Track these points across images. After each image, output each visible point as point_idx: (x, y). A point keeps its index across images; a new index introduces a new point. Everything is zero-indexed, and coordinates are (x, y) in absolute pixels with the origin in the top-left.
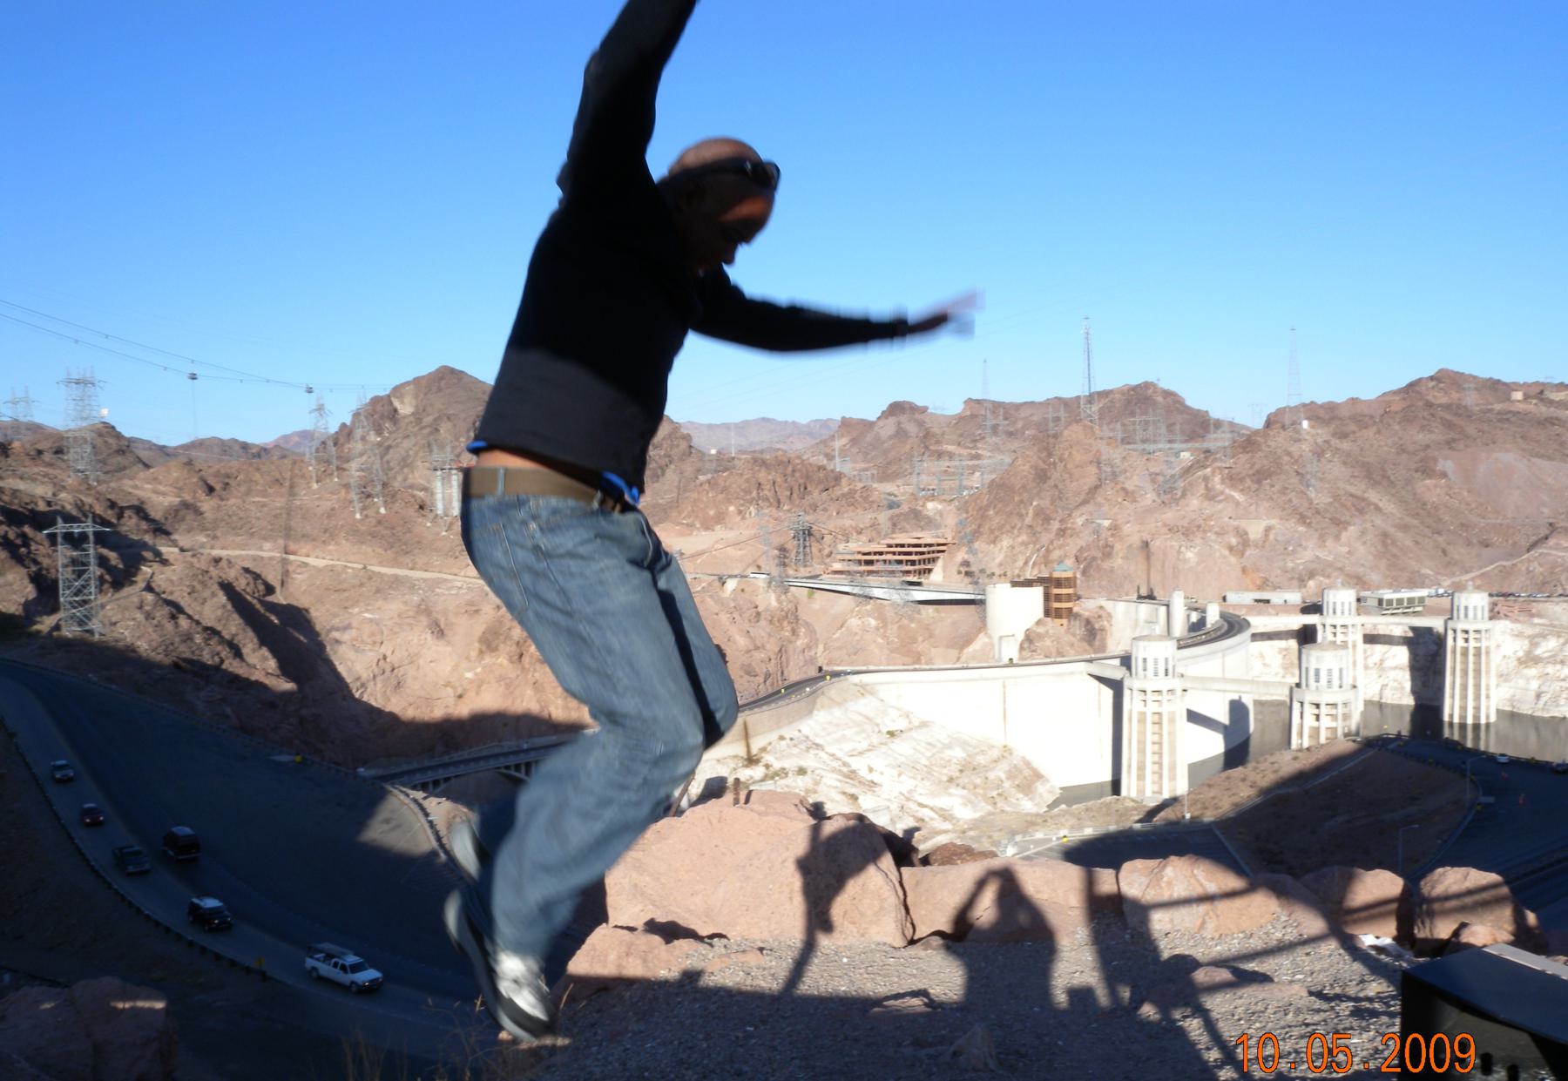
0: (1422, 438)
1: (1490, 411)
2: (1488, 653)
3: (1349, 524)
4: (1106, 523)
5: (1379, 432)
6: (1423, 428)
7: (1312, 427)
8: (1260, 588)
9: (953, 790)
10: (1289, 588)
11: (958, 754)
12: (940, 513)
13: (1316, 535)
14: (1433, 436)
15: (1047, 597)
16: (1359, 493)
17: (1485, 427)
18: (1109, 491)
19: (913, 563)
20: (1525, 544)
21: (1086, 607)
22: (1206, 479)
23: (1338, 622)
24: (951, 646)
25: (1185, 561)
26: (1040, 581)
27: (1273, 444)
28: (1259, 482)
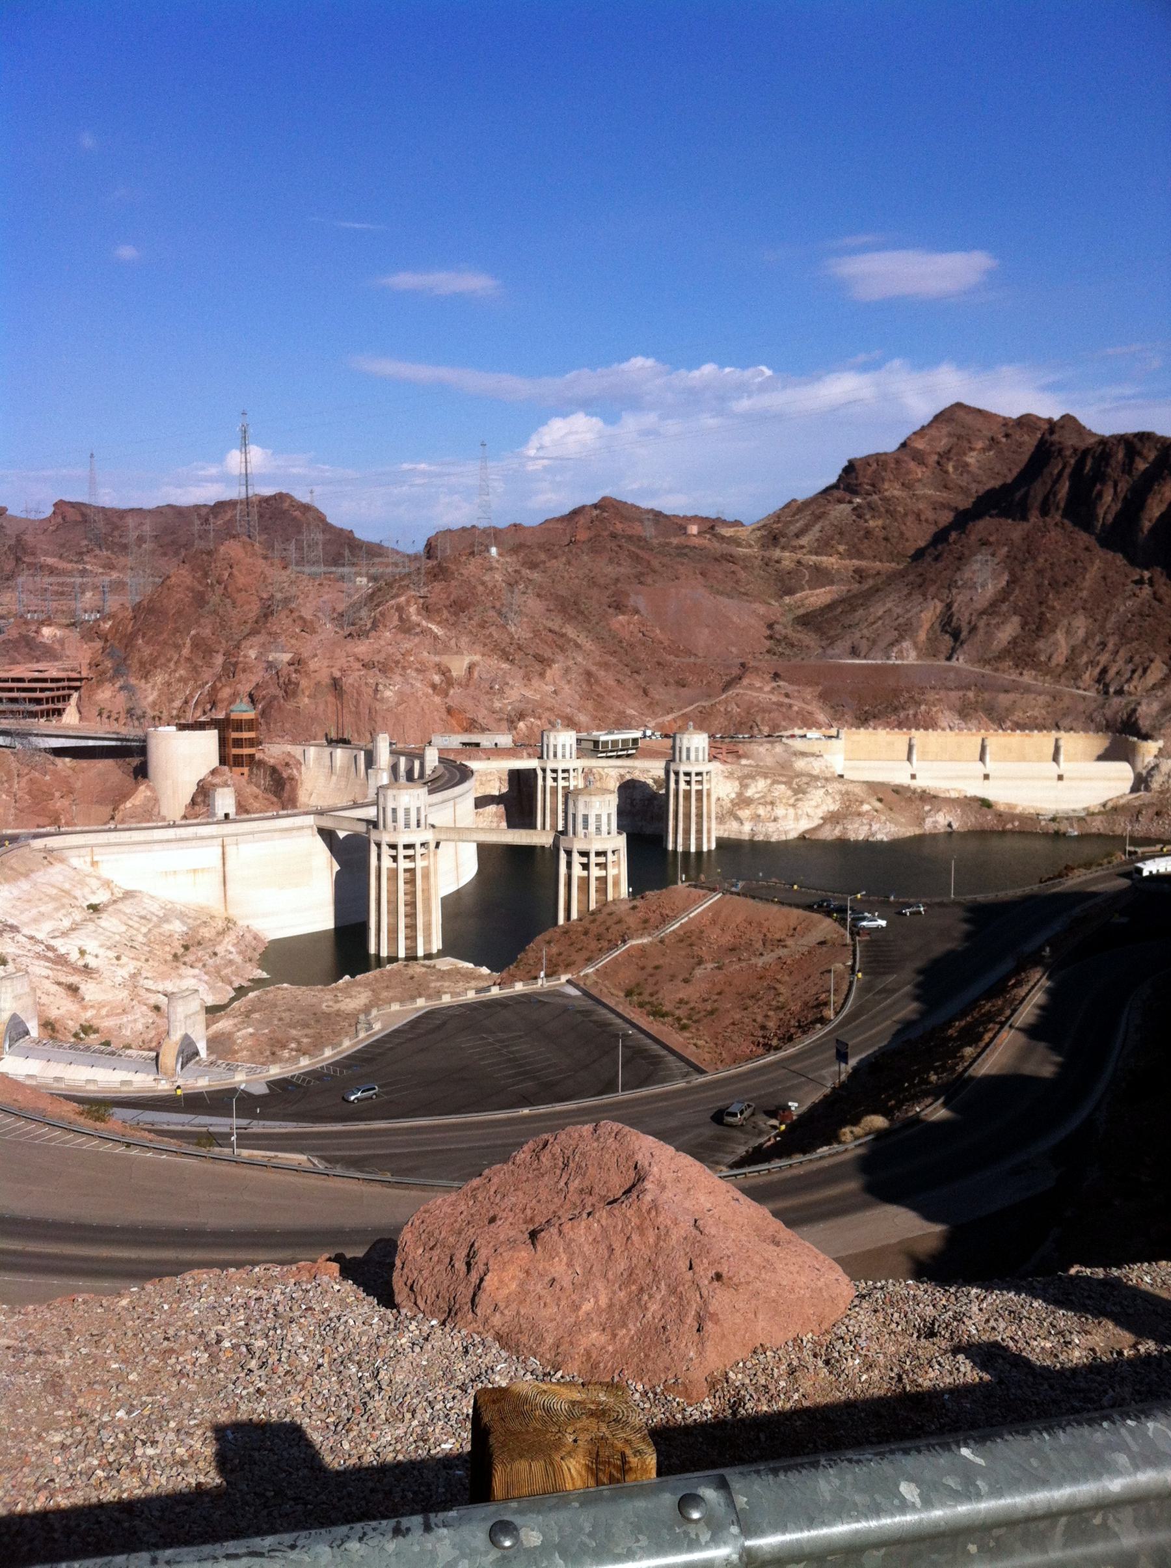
0: (611, 570)
1: (668, 544)
2: (709, 795)
3: (553, 661)
4: (286, 657)
5: (569, 563)
6: (611, 561)
7: (500, 555)
8: (467, 730)
9: (185, 971)
10: (499, 731)
11: (177, 927)
12: (62, 642)
13: (522, 672)
14: (622, 570)
15: (223, 742)
16: (556, 628)
17: (666, 560)
18: (281, 622)
19: (38, 701)
20: (719, 684)
21: (274, 751)
22: (400, 609)
23: (560, 766)
24: (101, 802)
25: (382, 700)
28: (456, 614)
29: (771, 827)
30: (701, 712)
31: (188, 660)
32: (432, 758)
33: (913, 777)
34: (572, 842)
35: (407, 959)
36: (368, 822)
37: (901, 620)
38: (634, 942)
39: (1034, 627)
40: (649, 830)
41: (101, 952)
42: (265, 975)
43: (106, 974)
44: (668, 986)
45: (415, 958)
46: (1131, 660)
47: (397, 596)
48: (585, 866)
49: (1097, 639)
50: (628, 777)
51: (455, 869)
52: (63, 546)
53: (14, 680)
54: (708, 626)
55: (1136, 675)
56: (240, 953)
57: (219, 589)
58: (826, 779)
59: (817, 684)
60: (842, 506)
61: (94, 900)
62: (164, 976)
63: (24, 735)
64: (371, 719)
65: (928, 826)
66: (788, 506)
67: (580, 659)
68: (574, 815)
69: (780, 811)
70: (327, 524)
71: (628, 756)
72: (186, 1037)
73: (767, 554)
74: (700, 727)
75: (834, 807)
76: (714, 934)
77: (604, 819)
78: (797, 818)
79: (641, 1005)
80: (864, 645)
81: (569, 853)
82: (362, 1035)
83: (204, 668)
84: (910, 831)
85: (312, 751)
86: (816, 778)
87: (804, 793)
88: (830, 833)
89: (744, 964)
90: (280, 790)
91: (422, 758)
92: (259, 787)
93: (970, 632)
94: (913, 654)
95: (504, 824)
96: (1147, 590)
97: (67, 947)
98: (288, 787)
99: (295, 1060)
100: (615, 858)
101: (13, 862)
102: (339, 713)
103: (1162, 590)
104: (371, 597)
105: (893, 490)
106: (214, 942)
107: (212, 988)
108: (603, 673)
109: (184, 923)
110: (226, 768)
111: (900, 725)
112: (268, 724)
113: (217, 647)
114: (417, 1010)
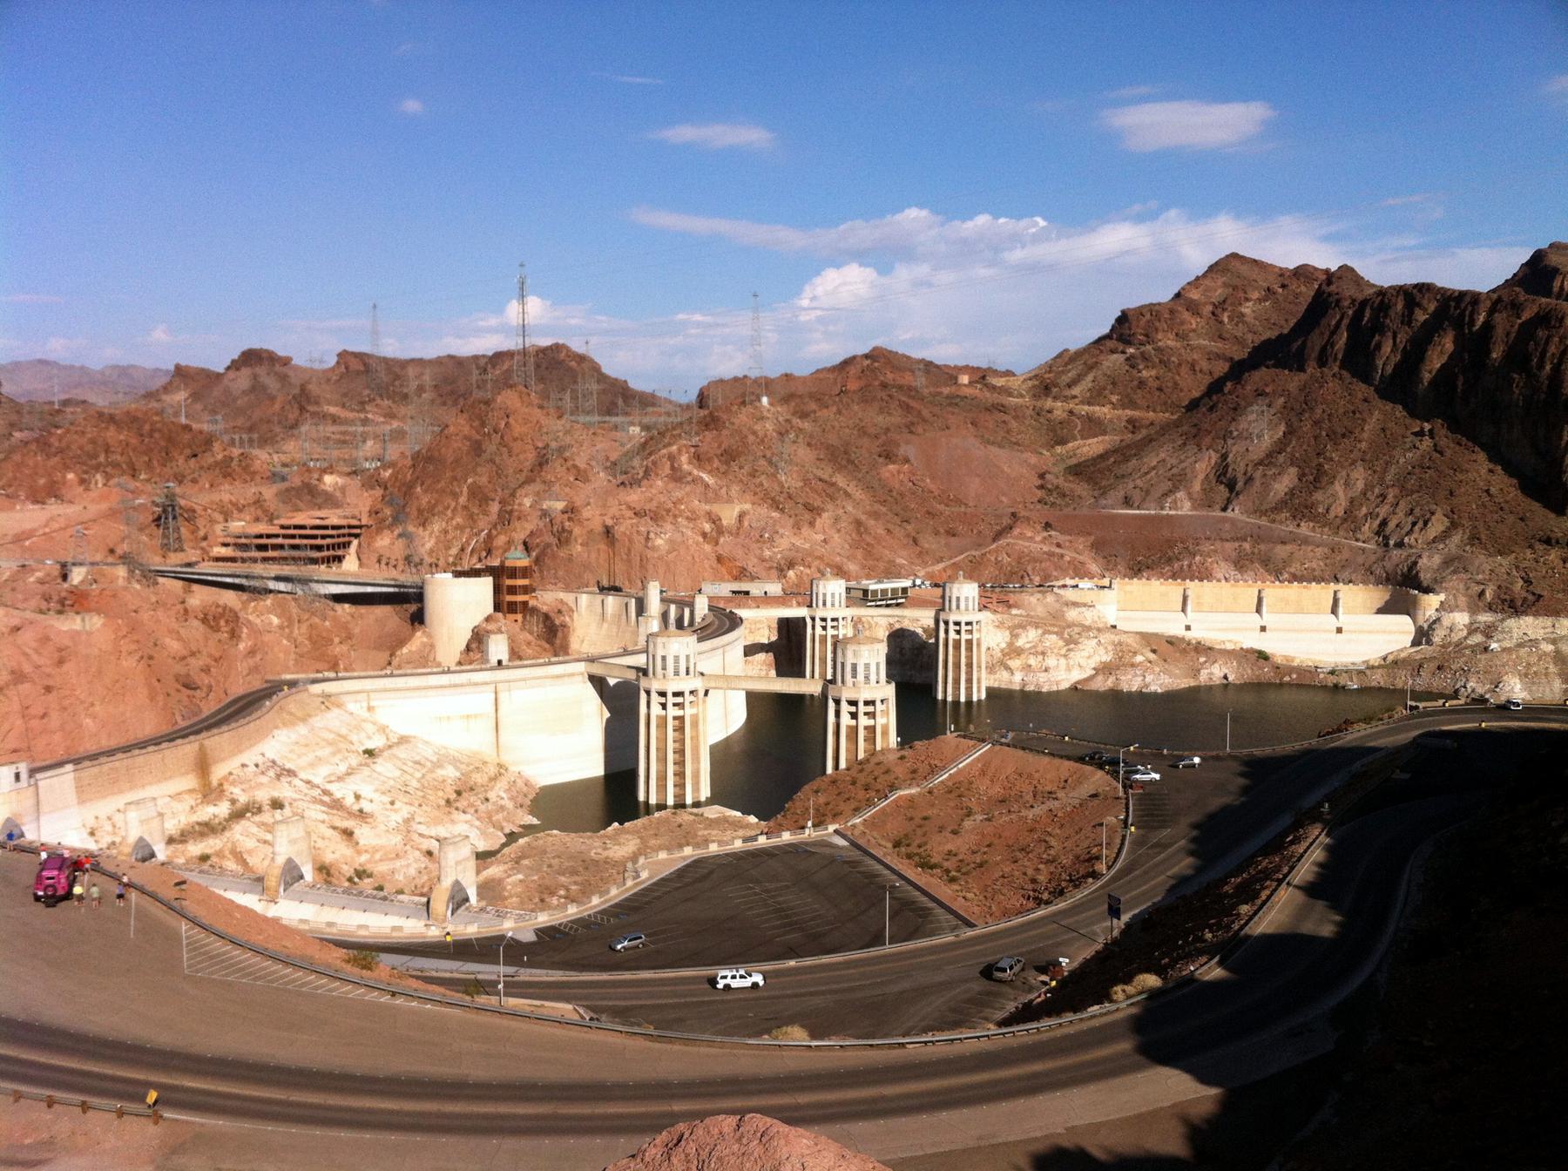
2: (979, 645)
3: (823, 510)
4: (560, 505)
5: (839, 412)
6: (881, 411)
7: (771, 404)
8: (736, 579)
10: (769, 579)
11: (450, 773)
12: (343, 489)
15: (497, 590)
16: (826, 477)
17: (936, 410)
18: (556, 470)
19: (319, 548)
21: (546, 599)
22: (672, 458)
23: (829, 615)
24: (378, 647)
25: (654, 549)
27: (736, 421)
28: (727, 463)
29: (1042, 677)
31: (465, 508)
32: (702, 606)
33: (1188, 628)
34: (840, 691)
35: (676, 806)
36: (638, 669)
37: (1175, 471)
38: (902, 793)
40: (919, 679)
41: (376, 796)
42: (535, 821)
43: (380, 819)
44: (937, 838)
45: (683, 806)
47: (670, 444)
48: (854, 716)
49: (1377, 491)
50: (897, 626)
51: (724, 717)
52: (345, 395)
53: (296, 527)
56: (512, 798)
57: (496, 438)
58: (1099, 630)
59: (1089, 534)
61: (370, 745)
62: (437, 822)
63: (304, 581)
64: (642, 566)
65: (1203, 678)
66: (1060, 356)
67: (850, 508)
69: (1051, 661)
70: (430, 361)
71: (898, 605)
72: (457, 883)
73: (1039, 404)
74: (970, 577)
75: (1106, 658)
76: (983, 785)
77: (873, 669)
78: (1069, 669)
79: (909, 856)
80: (1137, 496)
81: (837, 702)
82: (629, 883)
84: (1184, 683)
85: (584, 599)
86: (1089, 628)
87: (1076, 643)
88: (1103, 684)
89: (1013, 816)
90: (552, 636)
91: (691, 605)
92: (531, 633)
94: (1188, 504)
95: (773, 673)
96: (1427, 443)
97: (343, 791)
98: (560, 634)
99: (564, 907)
100: (884, 707)
101: (292, 707)
102: (610, 561)
104: (644, 445)
105: (1167, 341)
106: (486, 787)
107: (484, 833)
108: (872, 522)
109: (457, 768)
111: (1174, 577)
112: (541, 571)
113: (492, 495)
114: (684, 858)
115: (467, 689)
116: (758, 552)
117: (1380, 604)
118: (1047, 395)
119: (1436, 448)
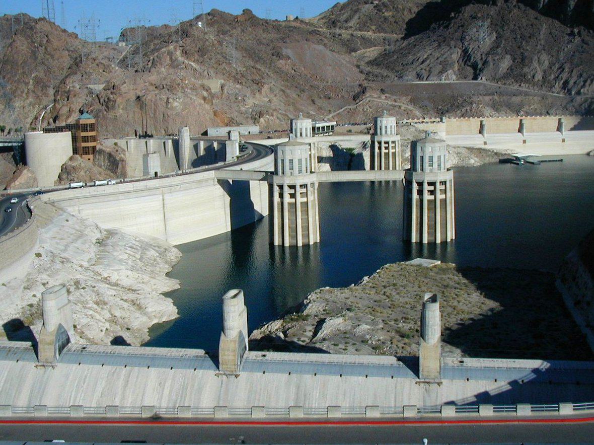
15: (74, 139)
21: (107, 144)
25: (172, 108)
26: (68, 127)
28: (202, 56)
30: (348, 112)
39: (520, 60)
46: (581, 75)
49: (557, 66)
54: (330, 65)
55: (587, 84)
57: (42, 50)
59: (407, 95)
60: (367, 5)
64: (164, 120)
66: (336, 6)
68: (422, 158)
73: (332, 31)
80: (425, 74)
83: (44, 97)
93: (483, 65)
94: (454, 77)
96: (577, 39)
98: (120, 166)
103: (587, 38)
108: (289, 91)
110: (78, 156)
111: (463, 116)
113: (49, 84)
115: (146, 193)
116: (237, 108)
117: (572, 126)
118: (335, 26)
119: (583, 41)
